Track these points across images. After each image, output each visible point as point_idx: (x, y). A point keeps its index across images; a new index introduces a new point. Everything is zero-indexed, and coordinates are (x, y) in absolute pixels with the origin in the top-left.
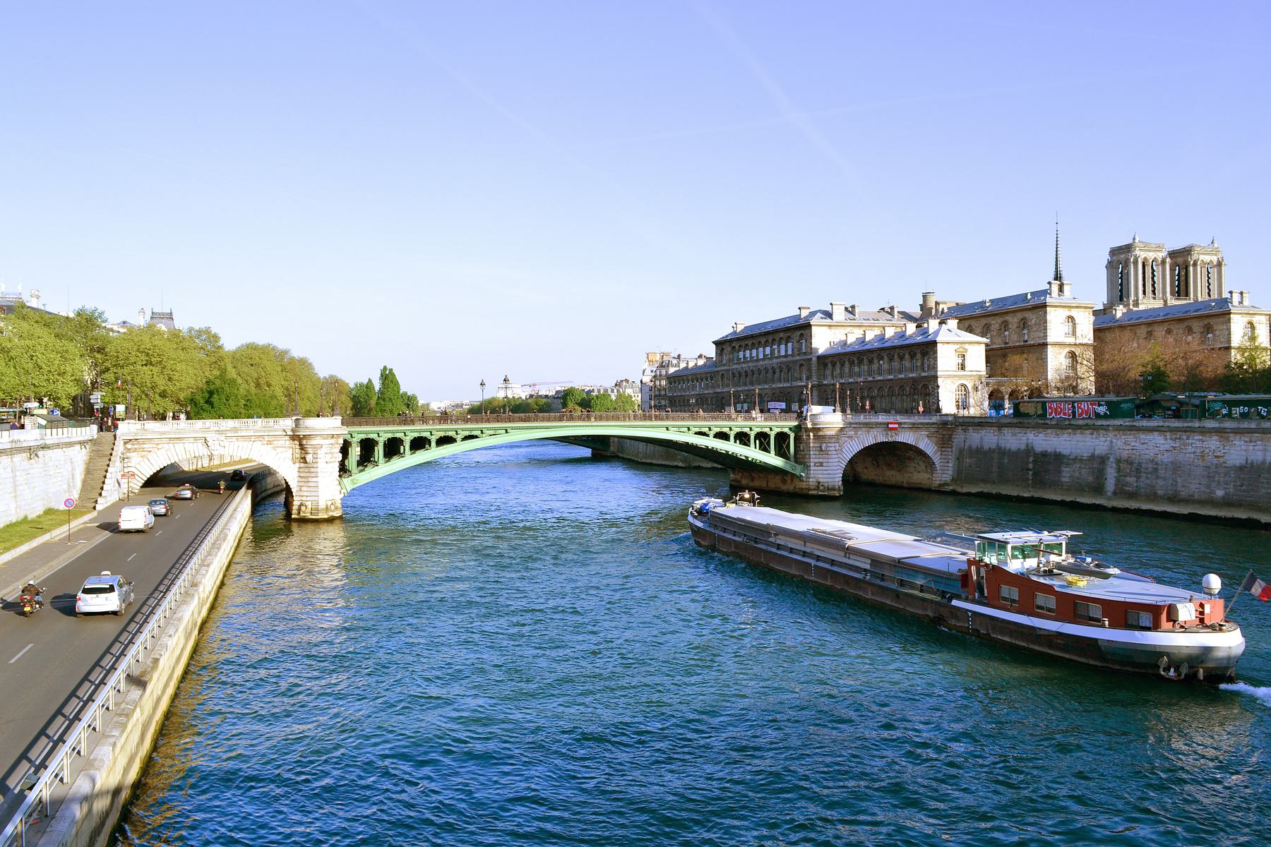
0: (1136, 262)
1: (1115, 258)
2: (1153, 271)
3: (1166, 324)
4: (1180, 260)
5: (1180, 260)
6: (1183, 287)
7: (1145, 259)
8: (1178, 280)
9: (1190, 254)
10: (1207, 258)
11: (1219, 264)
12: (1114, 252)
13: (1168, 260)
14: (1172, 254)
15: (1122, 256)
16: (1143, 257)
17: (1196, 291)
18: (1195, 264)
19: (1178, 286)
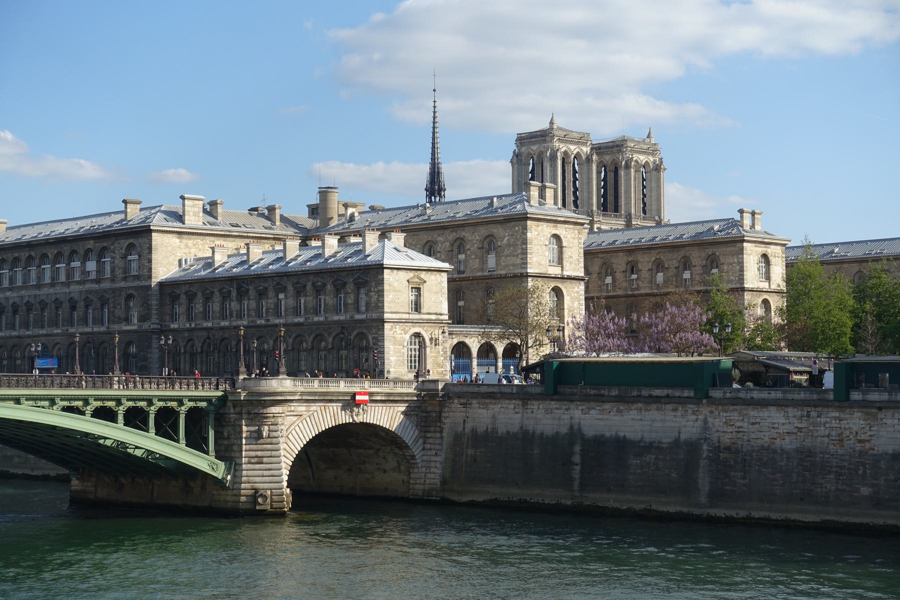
0: (553, 158)
1: (523, 149)
2: (575, 172)
4: (607, 158)
5: (607, 158)
6: (611, 198)
7: (566, 153)
8: (605, 187)
9: (620, 151)
10: (642, 159)
12: (523, 140)
13: (595, 157)
14: (599, 149)
15: (534, 148)
16: (563, 150)
17: (628, 203)
18: (628, 167)
19: (605, 196)
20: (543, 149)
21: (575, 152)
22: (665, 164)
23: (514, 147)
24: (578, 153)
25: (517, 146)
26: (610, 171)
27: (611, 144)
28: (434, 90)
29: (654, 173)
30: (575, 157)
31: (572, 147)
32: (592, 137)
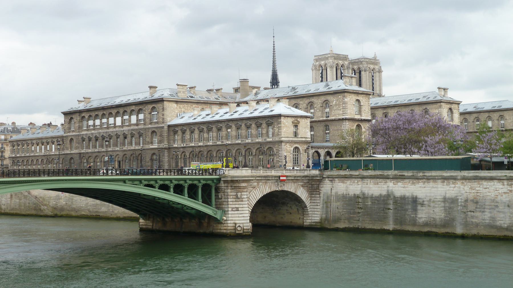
1: (317, 63)
3: (182, 126)
7: (337, 64)
11: (380, 71)
12: (318, 59)
13: (351, 66)
14: (353, 62)
20: (327, 63)
21: (341, 64)
22: (383, 69)
24: (343, 64)
26: (357, 73)
27: (357, 61)
28: (274, 37)
29: (377, 73)
30: (341, 66)
32: (349, 57)
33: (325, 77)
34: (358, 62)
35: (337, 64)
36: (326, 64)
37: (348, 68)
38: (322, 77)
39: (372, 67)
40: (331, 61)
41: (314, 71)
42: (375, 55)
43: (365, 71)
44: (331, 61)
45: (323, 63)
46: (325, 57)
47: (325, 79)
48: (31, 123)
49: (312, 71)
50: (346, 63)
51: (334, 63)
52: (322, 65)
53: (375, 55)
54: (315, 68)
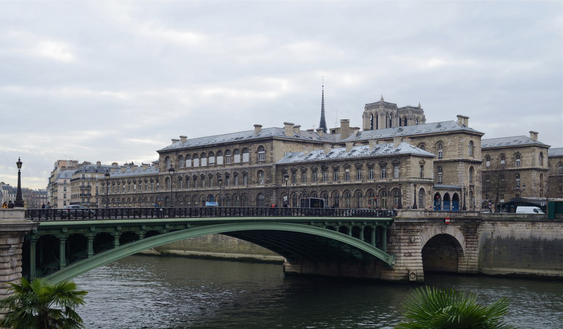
1: (368, 111)
20: (378, 111)
22: (426, 118)
23: (364, 110)
25: (366, 110)
28: (323, 86)
31: (390, 110)
33: (375, 124)
34: (405, 109)
35: (387, 112)
36: (377, 112)
37: (397, 116)
38: (372, 124)
39: (416, 115)
40: (382, 109)
41: (365, 119)
42: (419, 104)
43: (411, 119)
44: (381, 108)
45: (373, 111)
46: (375, 105)
47: (375, 127)
48: (114, 163)
49: (363, 118)
50: (395, 111)
51: (384, 111)
52: (373, 112)
53: (419, 104)
54: (365, 115)
